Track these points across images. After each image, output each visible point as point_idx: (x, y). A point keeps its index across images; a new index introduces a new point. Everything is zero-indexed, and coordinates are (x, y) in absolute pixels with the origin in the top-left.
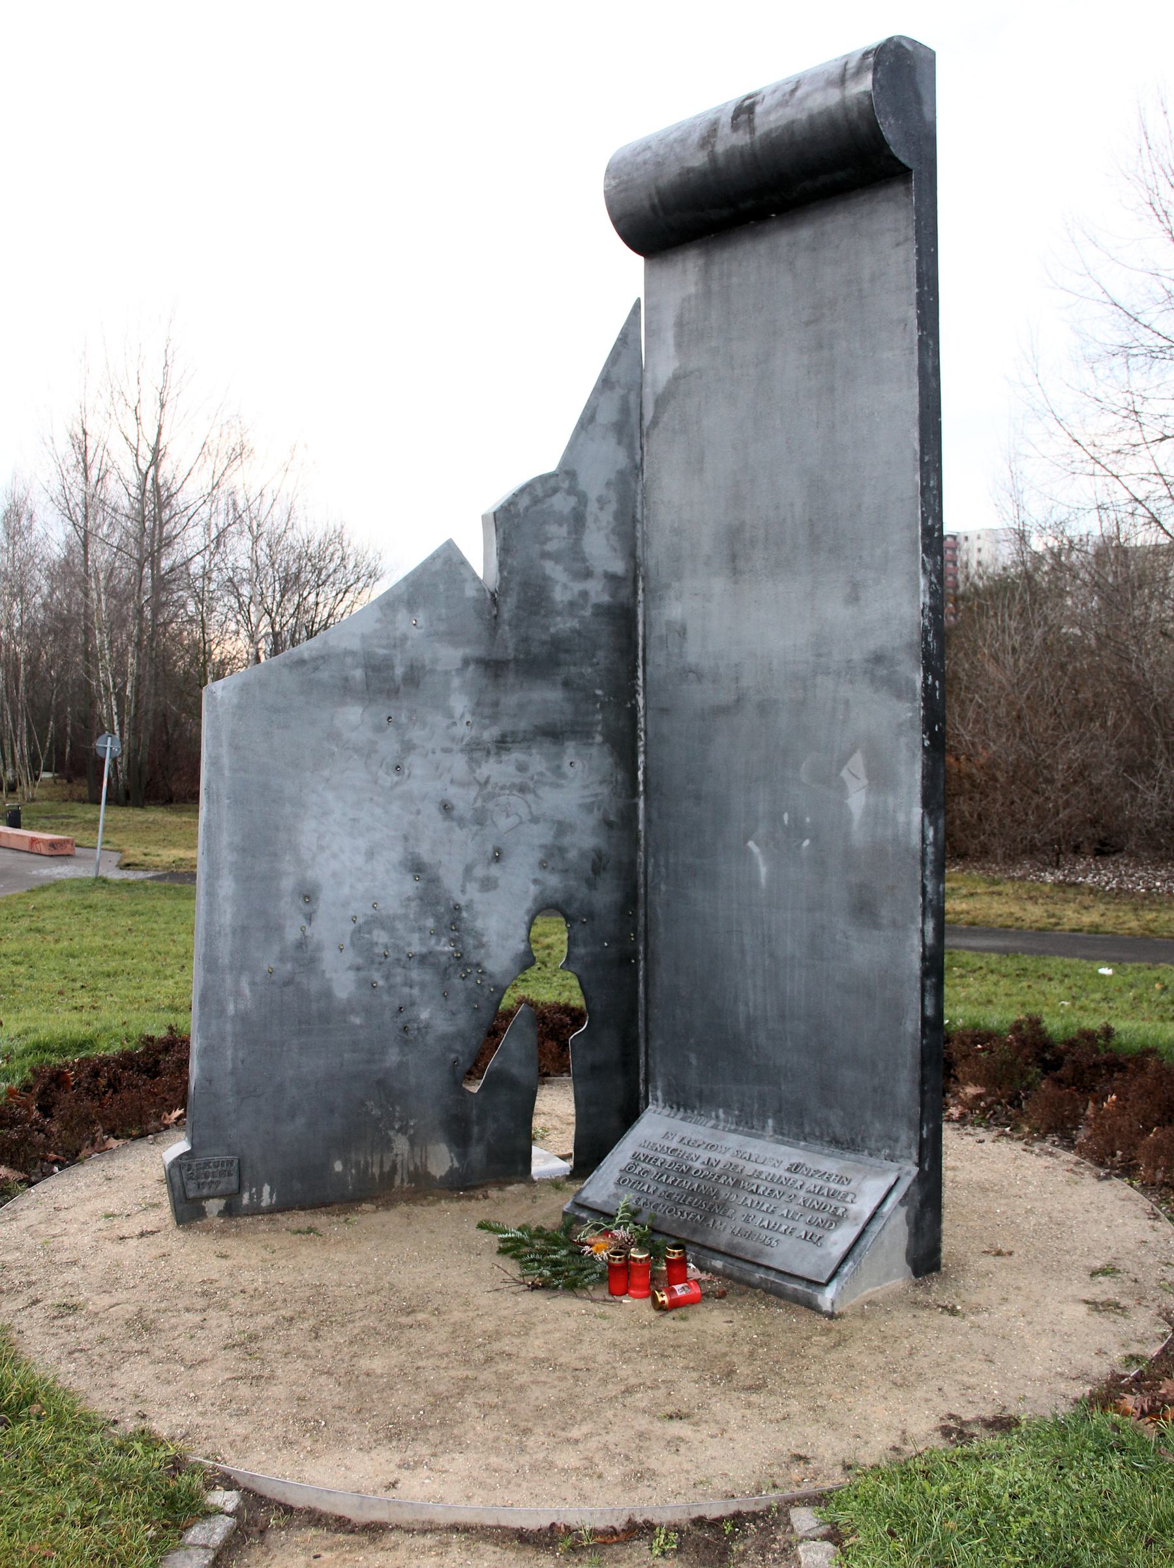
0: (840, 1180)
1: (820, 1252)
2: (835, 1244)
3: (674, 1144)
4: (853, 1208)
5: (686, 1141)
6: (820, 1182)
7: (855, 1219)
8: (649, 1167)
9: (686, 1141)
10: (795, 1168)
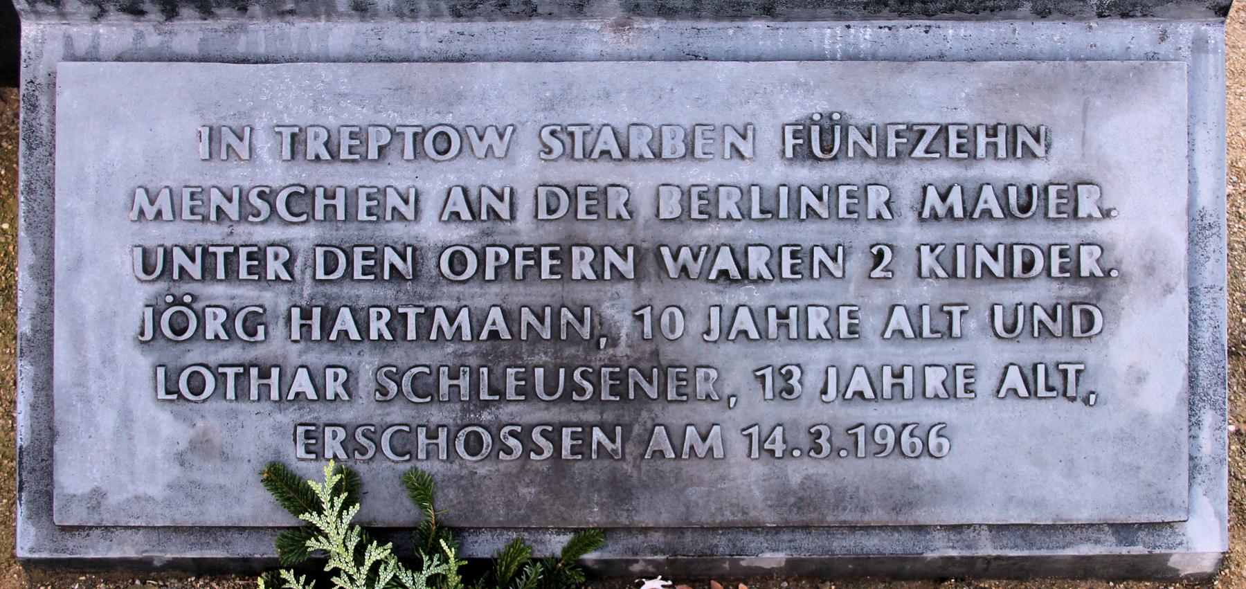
0: (1019, 141)
1: (1101, 420)
2: (1141, 379)
3: (276, 172)
4: (1122, 233)
5: (315, 147)
6: (942, 172)
7: (1150, 270)
8: (247, 294)
9: (315, 147)
10: (819, 139)
